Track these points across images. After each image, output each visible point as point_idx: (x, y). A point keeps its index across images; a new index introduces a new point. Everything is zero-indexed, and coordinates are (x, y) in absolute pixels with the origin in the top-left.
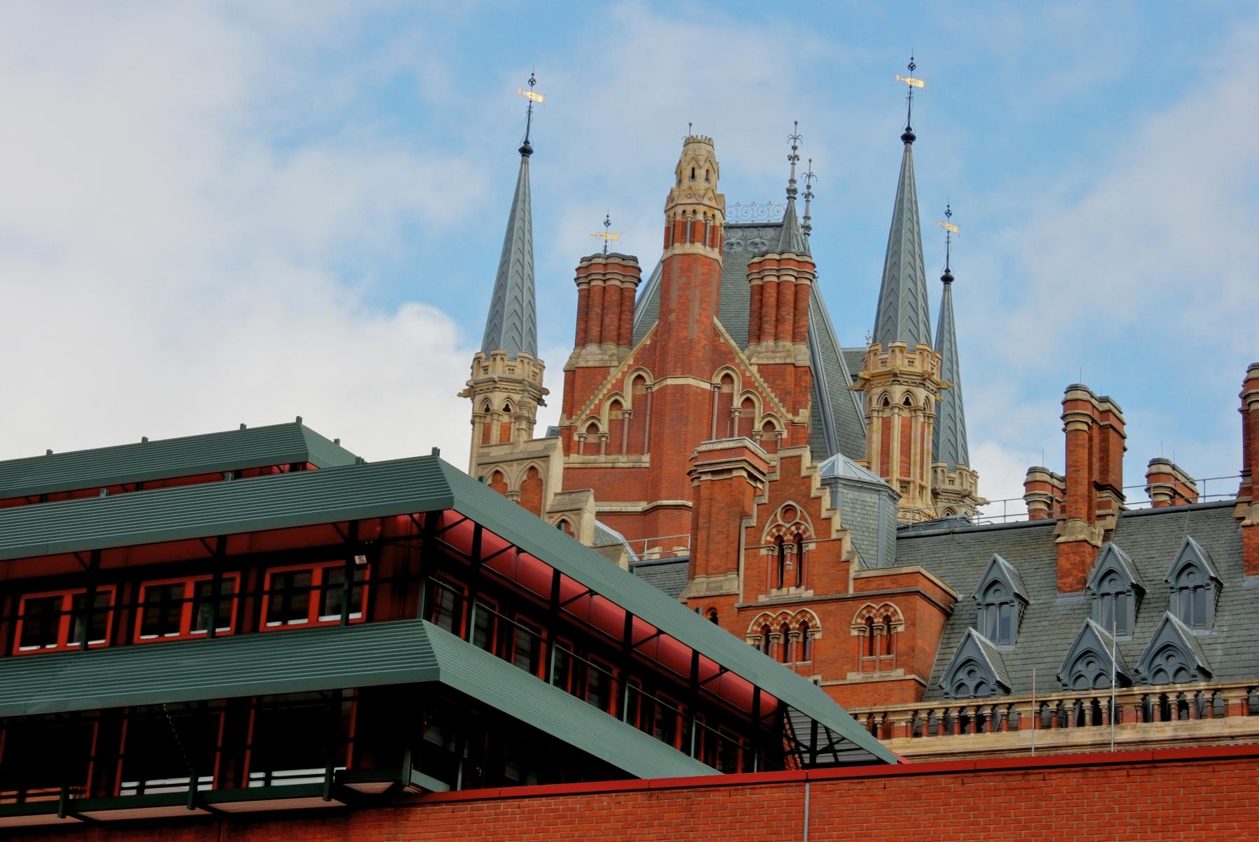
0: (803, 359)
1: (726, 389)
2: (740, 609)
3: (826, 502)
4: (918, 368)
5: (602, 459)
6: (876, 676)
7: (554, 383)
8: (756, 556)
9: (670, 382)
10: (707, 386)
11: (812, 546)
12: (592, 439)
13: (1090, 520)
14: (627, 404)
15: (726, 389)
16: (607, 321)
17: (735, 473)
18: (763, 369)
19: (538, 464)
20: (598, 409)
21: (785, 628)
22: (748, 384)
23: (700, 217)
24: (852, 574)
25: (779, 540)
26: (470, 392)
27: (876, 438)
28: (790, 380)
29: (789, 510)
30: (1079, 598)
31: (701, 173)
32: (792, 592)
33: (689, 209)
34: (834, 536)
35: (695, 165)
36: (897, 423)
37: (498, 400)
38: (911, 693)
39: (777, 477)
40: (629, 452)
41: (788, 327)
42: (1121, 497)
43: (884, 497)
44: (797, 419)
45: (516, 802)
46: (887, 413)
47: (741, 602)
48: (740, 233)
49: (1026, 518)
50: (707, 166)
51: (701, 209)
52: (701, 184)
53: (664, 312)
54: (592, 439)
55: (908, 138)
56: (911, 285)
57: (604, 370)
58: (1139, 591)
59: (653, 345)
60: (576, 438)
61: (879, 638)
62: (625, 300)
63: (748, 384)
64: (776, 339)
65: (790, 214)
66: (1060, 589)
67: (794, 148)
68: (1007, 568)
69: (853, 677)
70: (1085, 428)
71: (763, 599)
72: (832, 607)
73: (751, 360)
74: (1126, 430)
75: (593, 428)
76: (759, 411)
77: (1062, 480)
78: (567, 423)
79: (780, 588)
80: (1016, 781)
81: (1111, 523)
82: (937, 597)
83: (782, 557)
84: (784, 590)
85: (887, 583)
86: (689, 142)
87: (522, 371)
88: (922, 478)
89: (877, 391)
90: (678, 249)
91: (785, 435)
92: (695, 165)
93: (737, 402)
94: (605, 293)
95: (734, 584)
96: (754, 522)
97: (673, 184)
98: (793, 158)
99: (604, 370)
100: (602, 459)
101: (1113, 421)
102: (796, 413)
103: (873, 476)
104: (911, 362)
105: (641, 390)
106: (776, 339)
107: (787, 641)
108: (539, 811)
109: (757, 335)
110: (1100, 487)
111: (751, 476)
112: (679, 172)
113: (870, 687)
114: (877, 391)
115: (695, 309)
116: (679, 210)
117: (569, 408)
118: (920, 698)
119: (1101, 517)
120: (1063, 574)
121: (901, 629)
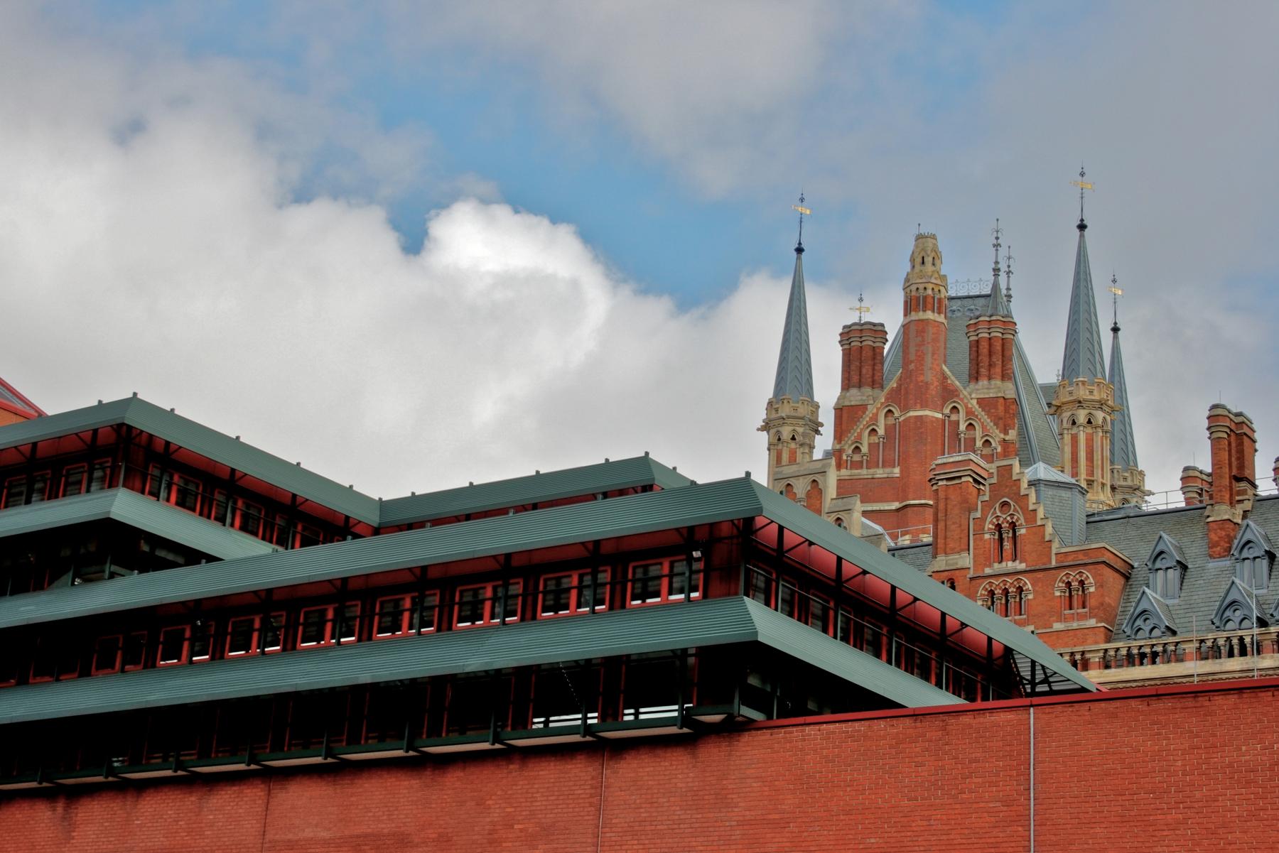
0: (1011, 394)
1: (954, 417)
3: (1033, 498)
4: (1096, 396)
5: (864, 473)
6: (1075, 625)
7: (827, 418)
8: (981, 539)
9: (912, 414)
10: (940, 416)
11: (1023, 531)
12: (857, 458)
13: (1232, 504)
14: (881, 431)
15: (954, 417)
16: (864, 371)
17: (964, 479)
18: (980, 401)
21: (1006, 592)
22: (970, 413)
23: (929, 292)
24: (1054, 551)
25: (999, 527)
26: (766, 427)
27: (1068, 449)
28: (1001, 408)
29: (1005, 504)
30: (1226, 563)
31: (929, 260)
32: (1010, 565)
33: (921, 287)
34: (1039, 523)
35: (925, 254)
37: (786, 432)
38: (1102, 637)
39: (994, 480)
40: (884, 466)
41: (998, 370)
42: (1255, 486)
44: (1007, 438)
45: (817, 727)
46: (1074, 431)
47: (971, 574)
48: (959, 302)
49: (1183, 505)
51: (930, 286)
52: (929, 267)
53: (906, 363)
54: (857, 458)
55: (1082, 227)
56: (1088, 335)
57: (863, 408)
58: (1271, 556)
59: (899, 386)
61: (1075, 597)
62: (876, 353)
63: (970, 413)
64: (990, 378)
65: (996, 287)
66: (1211, 556)
67: (997, 238)
69: (1058, 626)
71: (988, 571)
72: (1040, 575)
73: (972, 394)
74: (1256, 436)
75: (857, 449)
76: (978, 433)
77: (1209, 475)
78: (838, 447)
79: (1000, 562)
80: (1189, 702)
81: (1248, 505)
82: (1119, 565)
83: (1001, 539)
84: (1004, 564)
85: (1081, 556)
86: (920, 237)
87: (803, 410)
89: (1066, 415)
90: (914, 316)
91: (999, 450)
92: (925, 254)
93: (963, 427)
94: (861, 349)
95: (966, 560)
96: (978, 515)
97: (908, 269)
98: (997, 246)
99: (863, 408)
100: (864, 473)
101: (1246, 430)
102: (1006, 433)
103: (1066, 478)
104: (1091, 392)
105: (891, 421)
106: (990, 378)
107: (1007, 601)
108: (834, 733)
109: (975, 376)
110: (1238, 479)
111: (975, 480)
112: (912, 260)
113: (1071, 633)
114: (1066, 415)
115: (929, 359)
116: (914, 288)
117: (839, 435)
118: (1108, 640)
119: (1240, 501)
120: (1212, 545)
121: (1092, 589)
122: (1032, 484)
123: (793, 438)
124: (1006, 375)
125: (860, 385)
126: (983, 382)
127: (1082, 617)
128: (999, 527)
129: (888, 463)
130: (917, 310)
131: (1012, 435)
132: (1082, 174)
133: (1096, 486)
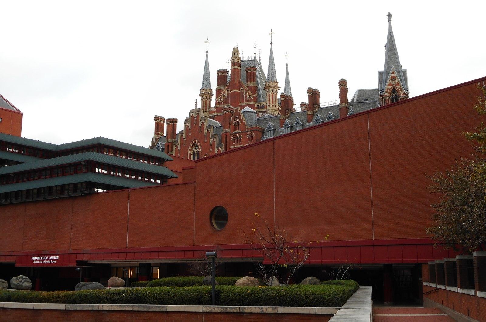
4: (274, 85)
7: (214, 93)
9: (232, 91)
11: (240, 123)
12: (221, 102)
13: (285, 115)
14: (226, 95)
17: (228, 112)
19: (198, 112)
20: (221, 97)
23: (236, 61)
26: (200, 95)
27: (268, 98)
29: (237, 117)
32: (238, 131)
33: (234, 60)
35: (236, 51)
36: (271, 95)
37: (204, 96)
41: (252, 79)
43: (254, 113)
48: (246, 62)
50: (237, 52)
51: (236, 60)
52: (236, 55)
54: (221, 102)
55: (271, 44)
56: (272, 70)
57: (222, 90)
60: (218, 102)
62: (225, 77)
63: (246, 90)
64: (250, 82)
65: (255, 58)
69: (247, 144)
70: (284, 100)
71: (233, 132)
75: (221, 100)
76: (248, 95)
86: (234, 48)
87: (208, 91)
91: (252, 99)
92: (236, 51)
93: (244, 94)
96: (231, 120)
104: (273, 84)
106: (250, 82)
107: (237, 139)
109: (247, 81)
110: (287, 109)
116: (232, 61)
117: (217, 97)
119: (287, 114)
120: (281, 125)
121: (254, 136)
122: (244, 112)
123: (206, 98)
124: (254, 81)
125: (221, 85)
126: (249, 83)
130: (233, 66)
133: (274, 106)
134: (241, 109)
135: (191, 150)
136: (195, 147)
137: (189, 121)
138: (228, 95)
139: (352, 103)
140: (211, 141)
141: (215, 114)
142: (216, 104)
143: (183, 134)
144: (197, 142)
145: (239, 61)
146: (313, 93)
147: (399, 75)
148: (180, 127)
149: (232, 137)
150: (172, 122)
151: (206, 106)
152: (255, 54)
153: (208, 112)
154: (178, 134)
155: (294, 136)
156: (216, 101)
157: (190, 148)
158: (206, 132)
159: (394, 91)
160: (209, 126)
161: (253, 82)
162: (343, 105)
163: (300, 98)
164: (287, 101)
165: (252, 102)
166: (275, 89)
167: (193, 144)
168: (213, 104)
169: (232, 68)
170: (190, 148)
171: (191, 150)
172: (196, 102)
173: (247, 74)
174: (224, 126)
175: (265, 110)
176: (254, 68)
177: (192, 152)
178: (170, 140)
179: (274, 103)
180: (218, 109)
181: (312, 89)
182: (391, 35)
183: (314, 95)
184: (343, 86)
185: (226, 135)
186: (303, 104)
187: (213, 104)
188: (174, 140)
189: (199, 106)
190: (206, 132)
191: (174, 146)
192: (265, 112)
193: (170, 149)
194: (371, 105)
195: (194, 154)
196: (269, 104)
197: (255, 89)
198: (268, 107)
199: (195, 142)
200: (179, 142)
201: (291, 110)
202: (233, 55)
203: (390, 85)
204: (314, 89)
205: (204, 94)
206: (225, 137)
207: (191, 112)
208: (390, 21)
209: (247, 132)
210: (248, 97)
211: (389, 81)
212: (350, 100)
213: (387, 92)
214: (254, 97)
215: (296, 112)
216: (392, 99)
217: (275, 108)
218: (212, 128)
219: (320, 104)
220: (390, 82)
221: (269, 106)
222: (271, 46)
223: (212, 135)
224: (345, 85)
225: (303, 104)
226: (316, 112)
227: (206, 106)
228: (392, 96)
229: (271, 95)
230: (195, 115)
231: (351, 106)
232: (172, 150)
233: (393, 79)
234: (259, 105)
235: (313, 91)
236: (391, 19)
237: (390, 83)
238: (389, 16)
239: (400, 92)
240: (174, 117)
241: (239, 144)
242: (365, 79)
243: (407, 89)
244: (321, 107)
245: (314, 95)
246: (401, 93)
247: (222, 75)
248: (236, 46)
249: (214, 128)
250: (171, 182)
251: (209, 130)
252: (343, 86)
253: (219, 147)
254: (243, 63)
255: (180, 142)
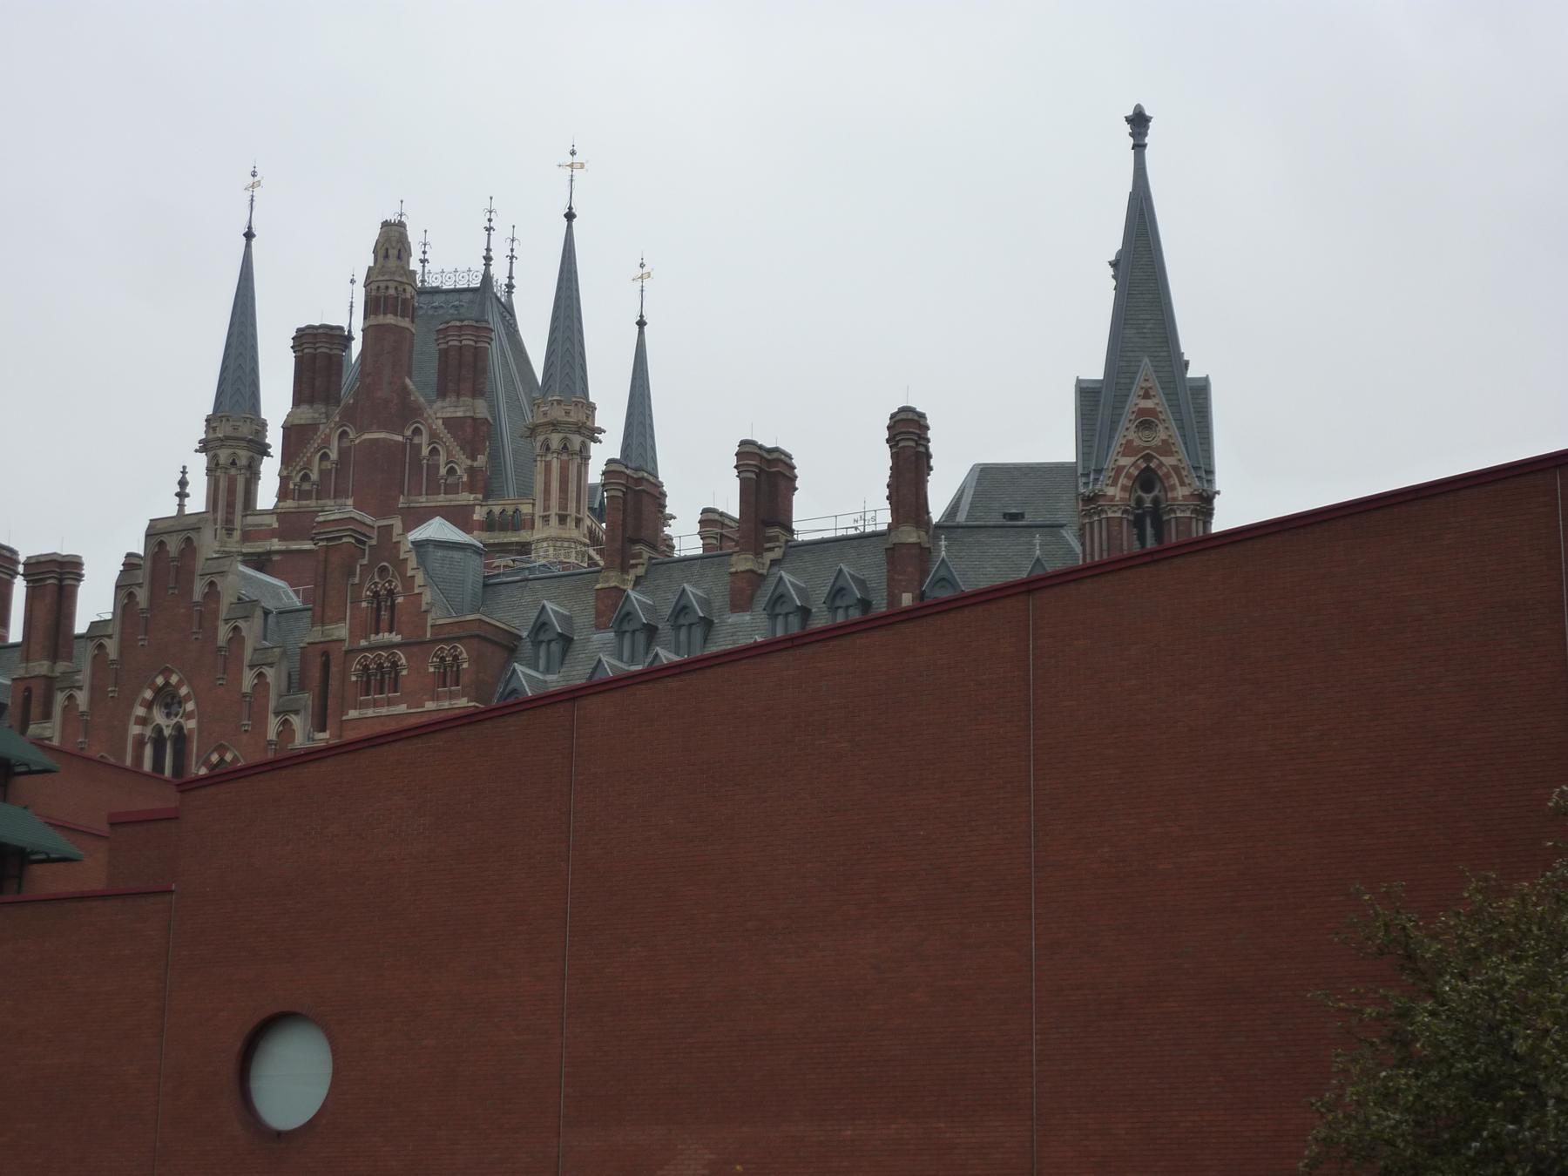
0: (481, 409)
1: (416, 440)
2: (347, 652)
7: (274, 438)
10: (400, 438)
12: (306, 486)
14: (334, 455)
15: (416, 440)
18: (446, 421)
19: (192, 534)
20: (310, 462)
21: (380, 666)
23: (392, 291)
25: (376, 594)
26: (205, 446)
29: (383, 570)
31: (393, 253)
32: (386, 637)
33: (382, 285)
35: (393, 242)
36: (555, 465)
37: (224, 455)
39: (374, 542)
47: (346, 646)
48: (443, 297)
52: (392, 263)
54: (306, 486)
55: (570, 216)
57: (312, 428)
61: (448, 675)
62: (334, 364)
63: (433, 436)
64: (458, 395)
65: (487, 278)
68: (555, 612)
71: (363, 643)
72: (415, 649)
73: (440, 411)
75: (305, 478)
76: (442, 458)
79: (377, 633)
83: (379, 609)
86: (385, 224)
87: (245, 430)
88: (578, 511)
89: (541, 438)
90: (373, 321)
91: (465, 479)
92: (393, 242)
93: (425, 451)
95: (341, 631)
96: (357, 580)
102: (474, 459)
104: (567, 413)
106: (458, 395)
109: (442, 393)
111: (358, 540)
114: (541, 438)
116: (374, 286)
120: (599, 615)
122: (418, 545)
123: (233, 463)
125: (311, 401)
126: (451, 399)
127: (452, 696)
128: (376, 594)
129: (339, 493)
131: (481, 460)
132: (573, 153)
133: (571, 523)
134: (408, 528)
135: (143, 721)
136: (167, 706)
137: (142, 576)
138: (342, 452)
139: (948, 526)
140: (248, 680)
141: (276, 545)
142: (283, 494)
143: (110, 637)
144: (180, 683)
145: (409, 289)
146: (761, 470)
147: (1175, 406)
148: (94, 603)
149: (355, 666)
150: (56, 578)
151: (230, 506)
152: (488, 259)
153: (237, 534)
154: (81, 637)
155: (674, 683)
156: (284, 480)
157: (140, 711)
158: (223, 632)
159: (1147, 480)
160: (246, 606)
161: (474, 396)
162: (910, 536)
163: (697, 488)
164: (636, 496)
165: (465, 498)
166: (576, 440)
167: (158, 691)
168: (267, 495)
169: (373, 321)
170: (140, 711)
171: (143, 721)
172: (183, 483)
173: (444, 354)
174: (320, 609)
175: (524, 536)
176: (481, 330)
177: (148, 732)
178: (41, 667)
179: (572, 506)
180: (288, 522)
181: (761, 447)
182: (1142, 215)
183: (766, 476)
184: (909, 438)
185: (326, 654)
186: (711, 521)
187: (267, 495)
188: (61, 667)
189: (197, 502)
190: (223, 632)
191: (60, 698)
192: (524, 548)
193: (36, 709)
194: (1037, 539)
195: (159, 742)
196: (546, 508)
197: (476, 434)
198: (538, 523)
199: (167, 683)
200: (84, 677)
201: (654, 547)
202: (380, 260)
203: (1128, 449)
204: (770, 451)
205: (224, 441)
206: (319, 660)
207: (157, 532)
208: (1139, 147)
209: (434, 642)
210: (443, 471)
211: (1127, 432)
212: (937, 507)
213: (1114, 484)
214: (471, 471)
215: (676, 554)
216: (1137, 516)
217: (575, 534)
218: (259, 613)
219: (795, 526)
220: (1132, 435)
221: (546, 519)
222: (569, 227)
223: (255, 650)
224: (920, 437)
225: (711, 521)
226: (774, 562)
227: (230, 506)
228: (1139, 501)
229: (555, 465)
230: (173, 545)
231: (943, 543)
232: (47, 716)
233: (1146, 422)
234: (497, 510)
235: (762, 457)
236: (1147, 140)
237: (1130, 442)
238: (1139, 122)
239: (1173, 488)
240: (65, 550)
241: (390, 703)
242: (1016, 413)
243: (1210, 472)
244: (800, 538)
245: (766, 476)
246: (1181, 492)
247: (317, 350)
248: (393, 218)
249: (266, 613)
250: (45, 881)
251: (241, 623)
252: (909, 438)
253: (287, 712)
254: (422, 298)
255: (94, 674)
